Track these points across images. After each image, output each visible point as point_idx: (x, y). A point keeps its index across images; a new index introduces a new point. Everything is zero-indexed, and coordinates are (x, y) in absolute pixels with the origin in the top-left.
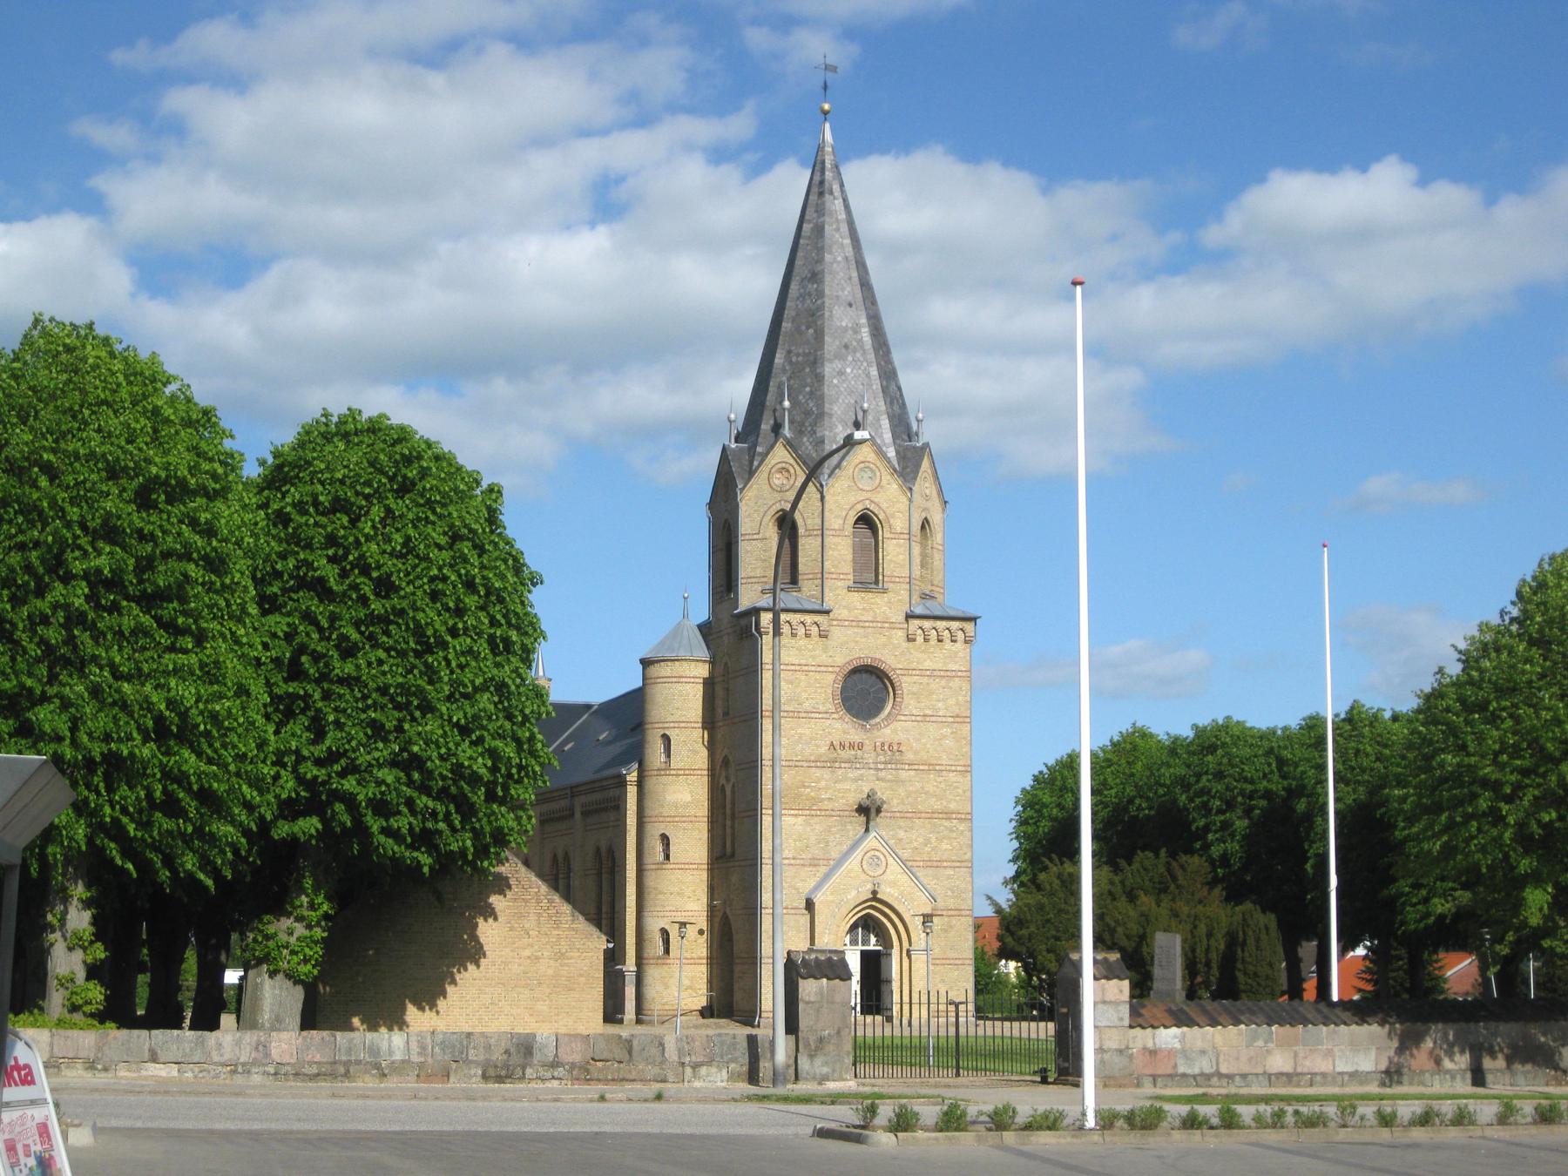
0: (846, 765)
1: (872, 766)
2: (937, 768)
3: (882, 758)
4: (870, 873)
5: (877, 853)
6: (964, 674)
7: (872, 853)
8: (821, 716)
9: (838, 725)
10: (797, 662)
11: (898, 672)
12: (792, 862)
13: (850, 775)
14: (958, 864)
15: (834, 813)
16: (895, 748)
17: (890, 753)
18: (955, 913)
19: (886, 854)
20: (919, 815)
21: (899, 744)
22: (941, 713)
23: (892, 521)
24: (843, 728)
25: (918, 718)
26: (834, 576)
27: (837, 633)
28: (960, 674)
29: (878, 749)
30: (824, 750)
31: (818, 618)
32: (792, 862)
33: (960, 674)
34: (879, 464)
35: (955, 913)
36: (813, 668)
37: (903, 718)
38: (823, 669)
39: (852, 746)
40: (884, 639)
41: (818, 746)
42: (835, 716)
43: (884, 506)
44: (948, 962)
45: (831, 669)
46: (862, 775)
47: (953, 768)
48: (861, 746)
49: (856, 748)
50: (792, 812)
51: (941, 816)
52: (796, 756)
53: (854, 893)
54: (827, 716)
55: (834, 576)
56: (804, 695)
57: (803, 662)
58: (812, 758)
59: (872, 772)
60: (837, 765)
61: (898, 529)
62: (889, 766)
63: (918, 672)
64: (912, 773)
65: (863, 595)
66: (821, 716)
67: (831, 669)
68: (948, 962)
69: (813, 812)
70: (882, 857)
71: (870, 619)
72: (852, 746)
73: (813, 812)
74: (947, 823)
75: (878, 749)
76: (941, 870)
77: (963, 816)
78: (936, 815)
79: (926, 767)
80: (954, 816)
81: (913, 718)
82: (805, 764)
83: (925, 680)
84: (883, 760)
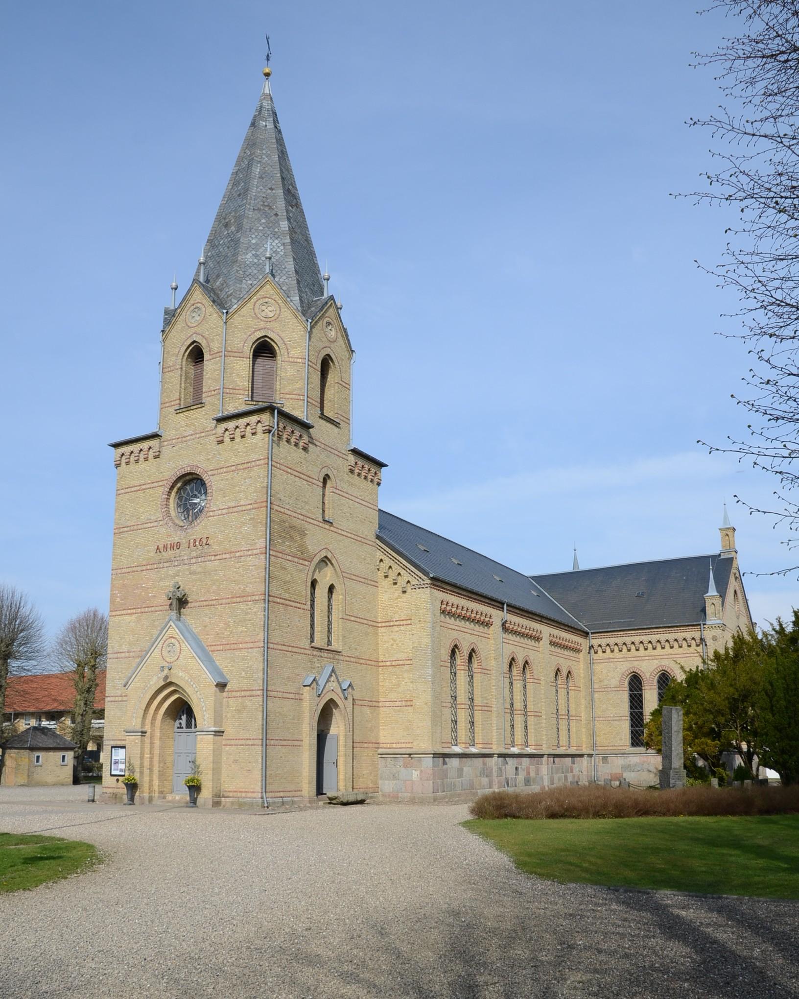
0: (168, 564)
1: (186, 562)
2: (237, 554)
3: (194, 554)
4: (168, 659)
5: (173, 640)
6: (262, 462)
7: (170, 641)
8: (152, 525)
9: (163, 530)
10: (138, 483)
11: (210, 473)
12: (127, 654)
13: (170, 573)
14: (251, 645)
15: (157, 609)
16: (204, 541)
17: (200, 548)
18: (247, 693)
19: (162, 642)
20: (220, 602)
21: (208, 538)
22: (242, 503)
23: (211, 344)
24: (167, 534)
25: (224, 511)
26: (167, 405)
27: (166, 451)
28: (258, 463)
29: (192, 544)
30: (152, 554)
31: (151, 443)
32: (127, 654)
33: (258, 463)
34: (204, 301)
35: (247, 693)
36: (148, 486)
37: (211, 514)
38: (155, 484)
39: (172, 547)
40: (200, 447)
41: (148, 551)
42: (161, 523)
43: (206, 334)
44: (241, 742)
45: (161, 483)
46: (179, 571)
47: (250, 552)
48: (178, 545)
49: (175, 548)
50: (129, 611)
51: (238, 600)
52: (134, 563)
53: (155, 678)
54: (156, 524)
55: (167, 405)
56: (142, 510)
57: (143, 482)
58: (144, 563)
59: (186, 567)
60: (161, 565)
61: (216, 350)
62: (199, 560)
63: (225, 470)
64: (217, 563)
65: (186, 413)
66: (152, 525)
67: (161, 483)
68: (241, 742)
69: (143, 610)
70: (177, 643)
71: (191, 432)
72: (172, 547)
73: (143, 610)
74: (243, 606)
75: (192, 544)
76: (237, 653)
77: (257, 598)
78: (235, 600)
79: (227, 556)
80: (249, 598)
81: (220, 512)
82: (139, 569)
83: (229, 476)
84: (195, 555)
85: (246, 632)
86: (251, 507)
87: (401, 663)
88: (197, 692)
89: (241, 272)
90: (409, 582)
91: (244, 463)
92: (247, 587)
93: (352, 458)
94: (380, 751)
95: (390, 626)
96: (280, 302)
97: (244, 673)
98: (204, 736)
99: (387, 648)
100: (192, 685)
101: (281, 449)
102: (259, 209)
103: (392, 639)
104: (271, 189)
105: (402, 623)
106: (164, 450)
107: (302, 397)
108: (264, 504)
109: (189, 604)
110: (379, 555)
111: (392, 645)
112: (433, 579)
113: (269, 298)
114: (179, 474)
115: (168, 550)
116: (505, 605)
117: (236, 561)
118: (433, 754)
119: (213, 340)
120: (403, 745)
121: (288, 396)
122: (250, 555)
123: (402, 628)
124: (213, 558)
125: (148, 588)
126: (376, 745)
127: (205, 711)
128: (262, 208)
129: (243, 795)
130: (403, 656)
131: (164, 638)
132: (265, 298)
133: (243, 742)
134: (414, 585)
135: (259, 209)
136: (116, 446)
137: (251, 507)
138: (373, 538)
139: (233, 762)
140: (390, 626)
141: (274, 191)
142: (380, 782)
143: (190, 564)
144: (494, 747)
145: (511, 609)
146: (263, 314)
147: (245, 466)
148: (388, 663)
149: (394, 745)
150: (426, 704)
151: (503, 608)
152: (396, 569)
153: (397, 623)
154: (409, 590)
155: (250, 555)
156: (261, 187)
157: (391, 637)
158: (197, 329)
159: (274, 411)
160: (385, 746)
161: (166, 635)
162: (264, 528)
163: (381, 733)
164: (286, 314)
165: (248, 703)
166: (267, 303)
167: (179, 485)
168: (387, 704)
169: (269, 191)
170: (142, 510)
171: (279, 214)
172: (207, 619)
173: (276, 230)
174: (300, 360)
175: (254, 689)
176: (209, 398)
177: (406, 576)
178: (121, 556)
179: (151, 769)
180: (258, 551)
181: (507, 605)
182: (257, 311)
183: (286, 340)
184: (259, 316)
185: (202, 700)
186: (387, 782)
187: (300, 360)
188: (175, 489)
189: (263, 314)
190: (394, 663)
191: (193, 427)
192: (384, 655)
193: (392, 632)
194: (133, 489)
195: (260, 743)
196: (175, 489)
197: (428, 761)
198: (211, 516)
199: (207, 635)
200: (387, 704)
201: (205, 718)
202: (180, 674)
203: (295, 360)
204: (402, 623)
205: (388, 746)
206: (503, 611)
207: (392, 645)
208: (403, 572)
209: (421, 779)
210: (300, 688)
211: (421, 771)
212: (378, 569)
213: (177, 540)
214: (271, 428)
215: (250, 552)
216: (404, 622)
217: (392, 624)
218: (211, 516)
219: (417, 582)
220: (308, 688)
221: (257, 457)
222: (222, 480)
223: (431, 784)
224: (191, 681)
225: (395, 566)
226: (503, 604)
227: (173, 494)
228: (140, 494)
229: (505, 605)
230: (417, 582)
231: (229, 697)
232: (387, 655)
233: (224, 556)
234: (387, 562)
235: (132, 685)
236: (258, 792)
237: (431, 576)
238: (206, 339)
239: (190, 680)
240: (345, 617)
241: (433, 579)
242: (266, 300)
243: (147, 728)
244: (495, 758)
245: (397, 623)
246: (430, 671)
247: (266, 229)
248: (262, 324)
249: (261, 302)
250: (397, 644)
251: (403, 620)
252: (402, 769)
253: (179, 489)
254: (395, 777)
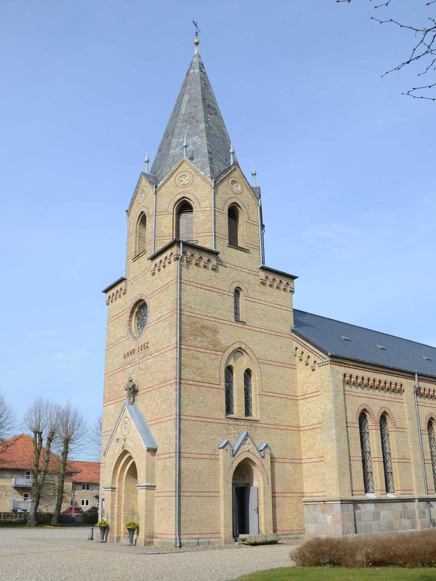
3: (141, 356)
9: (127, 343)
20: (154, 388)
28: (172, 283)
30: (122, 360)
36: (121, 314)
42: (126, 337)
47: (168, 349)
49: (132, 353)
56: (118, 331)
58: (119, 367)
59: (137, 366)
63: (156, 293)
64: (152, 360)
71: (140, 272)
76: (162, 425)
85: (167, 408)
86: (168, 315)
87: (315, 426)
88: (138, 456)
89: (171, 161)
90: (315, 362)
91: (165, 285)
92: (167, 374)
93: (263, 275)
94: (304, 499)
95: (306, 398)
96: (193, 172)
97: (165, 440)
98: (141, 490)
99: (305, 416)
100: (135, 452)
101: (190, 271)
102: (186, 121)
103: (308, 408)
104: (195, 107)
105: (313, 395)
106: (128, 289)
107: (211, 234)
108: (175, 311)
109: (139, 392)
110: (295, 344)
111: (308, 413)
112: (331, 356)
113: (185, 172)
114: (134, 302)
115: (129, 355)
116: (416, 375)
117: (162, 356)
118: (341, 501)
119: (150, 208)
120: (320, 494)
121: (200, 234)
122: (168, 351)
123: (314, 398)
124: (150, 357)
125: (120, 384)
126: (300, 495)
127: (142, 470)
128: (188, 119)
129: (166, 536)
130: (315, 421)
131: (123, 418)
132: (182, 172)
133: (165, 494)
134: (319, 364)
135: (186, 121)
136: (106, 291)
137: (168, 315)
138: (289, 332)
139: (160, 510)
140: (306, 398)
141: (197, 108)
142: (306, 525)
143: (139, 364)
144: (415, 493)
145: (422, 378)
146: (182, 183)
147: (165, 287)
148: (306, 428)
149: (314, 494)
150: (333, 458)
151: (414, 378)
152: (307, 353)
153: (310, 395)
154: (317, 368)
155: (168, 351)
156: (189, 108)
157: (307, 407)
158: (143, 204)
159: (180, 244)
160: (308, 495)
161: (123, 416)
162: (175, 329)
163: (305, 485)
164: (197, 180)
165: (168, 464)
166: (184, 175)
167: (136, 310)
168: (308, 461)
169: (194, 108)
170: (118, 331)
171: (199, 120)
172: (147, 402)
173: (197, 130)
174: (209, 209)
175: (171, 451)
176: (148, 247)
177: (313, 358)
178: (108, 364)
179: (119, 516)
180: (171, 347)
181: (418, 375)
182: (177, 182)
183: (198, 196)
184: (179, 185)
185: (140, 462)
186: (310, 525)
187: (209, 209)
188: (135, 314)
189: (182, 183)
190: (310, 427)
191: (141, 268)
192: (303, 422)
193: (307, 403)
194: (114, 318)
195: (174, 495)
196: (135, 314)
197: (337, 507)
198: (149, 327)
199: (148, 413)
200: (308, 461)
201: (142, 476)
202: (130, 444)
203: (205, 209)
204: (313, 395)
205: (310, 495)
206: (415, 380)
207: (308, 413)
208: (311, 355)
209: (333, 522)
210: (215, 451)
211: (333, 516)
212: (295, 355)
213: (133, 347)
214: (178, 256)
215: (168, 349)
216: (315, 394)
217: (307, 396)
218: (149, 327)
219: (320, 361)
220: (222, 450)
221: (171, 279)
222: (155, 300)
223: (341, 527)
224: (135, 448)
225: (305, 351)
226: (414, 374)
227: (134, 316)
228: (117, 320)
229: (416, 375)
230: (320, 361)
231: (158, 460)
232: (305, 421)
233: (156, 354)
234: (301, 349)
235: (107, 454)
236: (173, 534)
237: (330, 354)
238: (147, 208)
239: (134, 448)
240: (262, 393)
241: (331, 356)
242: (183, 173)
243: (116, 485)
244: (416, 503)
245: (310, 395)
246: (334, 431)
247: (190, 131)
248: (181, 190)
249: (180, 175)
250: (311, 412)
251: (314, 393)
252: (320, 514)
253: (137, 313)
254: (315, 521)
